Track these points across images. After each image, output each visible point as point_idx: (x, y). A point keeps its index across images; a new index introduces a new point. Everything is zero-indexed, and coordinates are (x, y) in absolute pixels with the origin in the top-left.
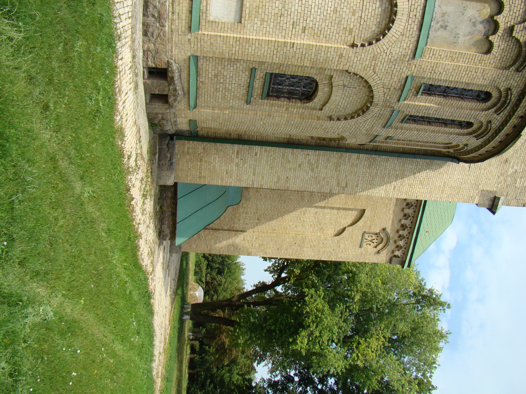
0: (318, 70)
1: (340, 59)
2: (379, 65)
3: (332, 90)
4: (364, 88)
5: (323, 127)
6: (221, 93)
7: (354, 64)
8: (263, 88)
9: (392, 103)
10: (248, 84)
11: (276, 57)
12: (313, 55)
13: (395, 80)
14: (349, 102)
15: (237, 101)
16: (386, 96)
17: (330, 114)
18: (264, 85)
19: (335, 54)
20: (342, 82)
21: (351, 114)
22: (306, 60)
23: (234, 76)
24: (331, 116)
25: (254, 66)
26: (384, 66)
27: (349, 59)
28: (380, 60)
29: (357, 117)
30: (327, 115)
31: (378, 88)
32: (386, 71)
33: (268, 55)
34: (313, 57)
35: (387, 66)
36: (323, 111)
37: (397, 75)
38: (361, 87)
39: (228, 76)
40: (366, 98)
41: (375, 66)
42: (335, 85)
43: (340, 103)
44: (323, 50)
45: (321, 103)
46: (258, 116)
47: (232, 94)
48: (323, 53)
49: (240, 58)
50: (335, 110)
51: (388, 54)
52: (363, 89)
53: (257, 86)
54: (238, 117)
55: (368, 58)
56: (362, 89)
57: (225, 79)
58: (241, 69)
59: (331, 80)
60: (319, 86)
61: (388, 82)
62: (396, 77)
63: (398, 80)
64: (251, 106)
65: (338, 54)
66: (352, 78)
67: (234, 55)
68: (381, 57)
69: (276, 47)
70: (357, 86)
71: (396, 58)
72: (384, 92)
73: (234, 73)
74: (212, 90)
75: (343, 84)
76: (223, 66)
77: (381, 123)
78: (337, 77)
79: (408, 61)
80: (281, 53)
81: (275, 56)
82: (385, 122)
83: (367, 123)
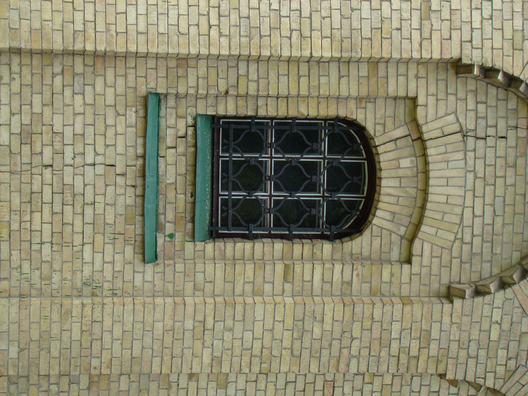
0: (364, 81)
1: (426, 23)
3: (426, 163)
5: (434, 346)
6: (47, 217)
7: (477, 34)
8: (194, 184)
10: (140, 162)
11: (221, 35)
12: (336, 16)
14: (499, 201)
15: (109, 248)
17: (445, 280)
18: (195, 166)
21: (519, 263)
22: (316, 35)
23: (90, 130)
24: (449, 288)
25: (152, 85)
27: (456, 18)
30: (435, 286)
33: (193, 30)
34: (336, 25)
39: (68, 131)
42: (434, 134)
43: (468, 213)
45: (402, 231)
46: (190, 310)
47: (89, 211)
49: (101, 48)
53: (170, 179)
54: (117, 332)
57: (58, 146)
58: (110, 100)
59: (415, 120)
60: (380, 149)
64: (159, 269)
66: (481, 97)
67: (80, 39)
73: (89, 119)
74: (16, 201)
75: (455, 127)
76: (47, 96)
80: (234, 17)
81: (214, 32)
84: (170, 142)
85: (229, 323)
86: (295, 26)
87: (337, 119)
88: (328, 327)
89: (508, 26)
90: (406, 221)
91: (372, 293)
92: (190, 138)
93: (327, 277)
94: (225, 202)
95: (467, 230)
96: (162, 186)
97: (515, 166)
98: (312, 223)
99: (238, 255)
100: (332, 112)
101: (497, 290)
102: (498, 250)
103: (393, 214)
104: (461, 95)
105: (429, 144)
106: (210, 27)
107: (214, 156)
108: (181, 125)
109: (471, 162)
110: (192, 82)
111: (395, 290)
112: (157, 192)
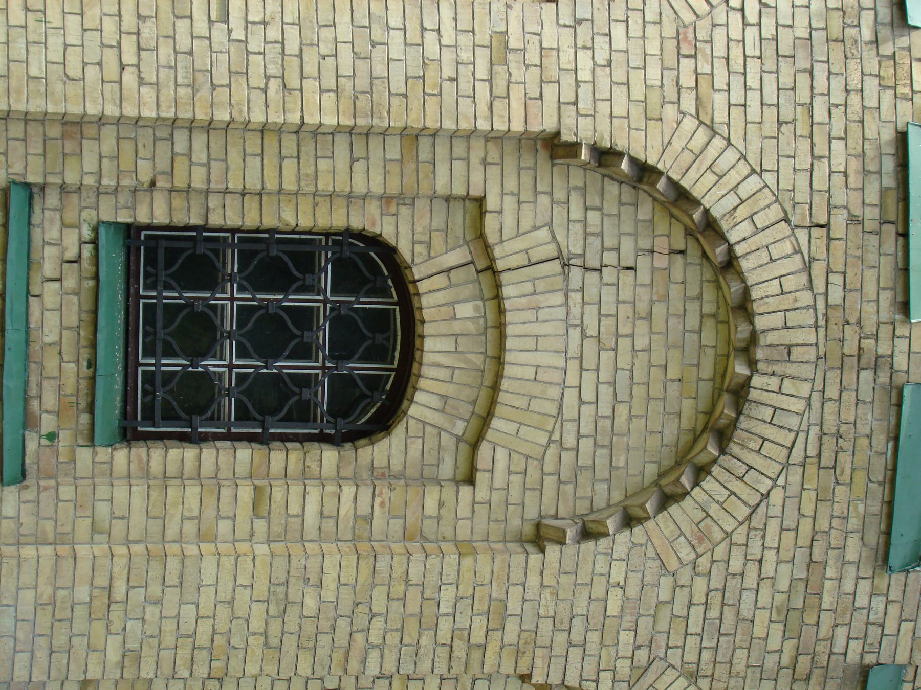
0: (394, 168)
1: (499, 69)
2: (720, 82)
3: (501, 311)
4: (679, 258)
5: (512, 626)
7: (585, 91)
8: (94, 345)
9: (869, 328)
11: (141, 82)
13: (838, 163)
14: (623, 376)
16: (820, 286)
17: (532, 513)
18: (95, 312)
19: (465, 40)
20: (544, 234)
21: (656, 484)
22: (310, 86)
24: (538, 526)
25: (17, 168)
26: (754, 82)
27: (550, 62)
28: (720, 50)
29: (696, 483)
31: (757, 231)
32: (770, 114)
33: (92, 73)
35: (769, 79)
36: (481, 478)
37: (838, 131)
38: (661, 262)
40: (709, 336)
41: (704, 83)
42: (513, 261)
43: (571, 398)
44: (395, 20)
45: (459, 427)
46: (84, 567)
48: (396, 37)
50: (549, 467)
51: (752, 17)
52: (677, 275)
55: (653, 48)
56: (668, 269)
59: (481, 236)
60: (423, 287)
61: (802, 181)
62: (838, 146)
63: (854, 165)
64: (30, 495)
65: (483, 37)
68: (719, 35)
69: (129, 21)
70: (638, 251)
71: (802, 33)
72: (798, 251)
75: (551, 250)
77: (854, 523)
78: (510, 203)
79: (876, 42)
80: (165, 51)
81: (129, 78)
82: (876, 507)
83: (772, 540)
84: (49, 269)
85: (155, 589)
86: (273, 70)
87: (349, 233)
88: (329, 595)
89: (636, 78)
90: (465, 410)
91: (407, 536)
92: (86, 264)
93: (329, 508)
94: (149, 377)
95: (570, 427)
96: (35, 347)
97: (649, 317)
98: (303, 414)
99: (172, 470)
100: (339, 221)
101: (618, 530)
102: (620, 461)
103: (444, 398)
104: (560, 195)
105: (505, 278)
106: (122, 68)
107: (131, 296)
108: (71, 241)
109: (575, 311)
110: (90, 164)
111: (447, 531)
112: (27, 359)
